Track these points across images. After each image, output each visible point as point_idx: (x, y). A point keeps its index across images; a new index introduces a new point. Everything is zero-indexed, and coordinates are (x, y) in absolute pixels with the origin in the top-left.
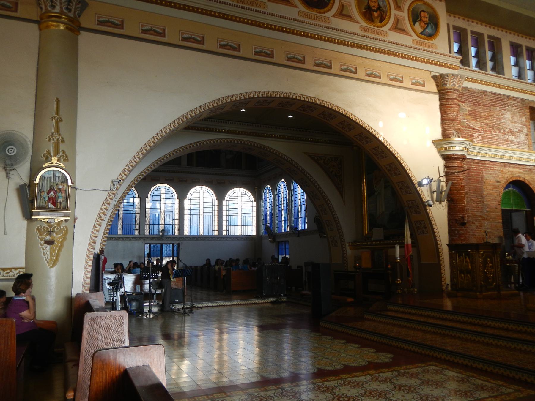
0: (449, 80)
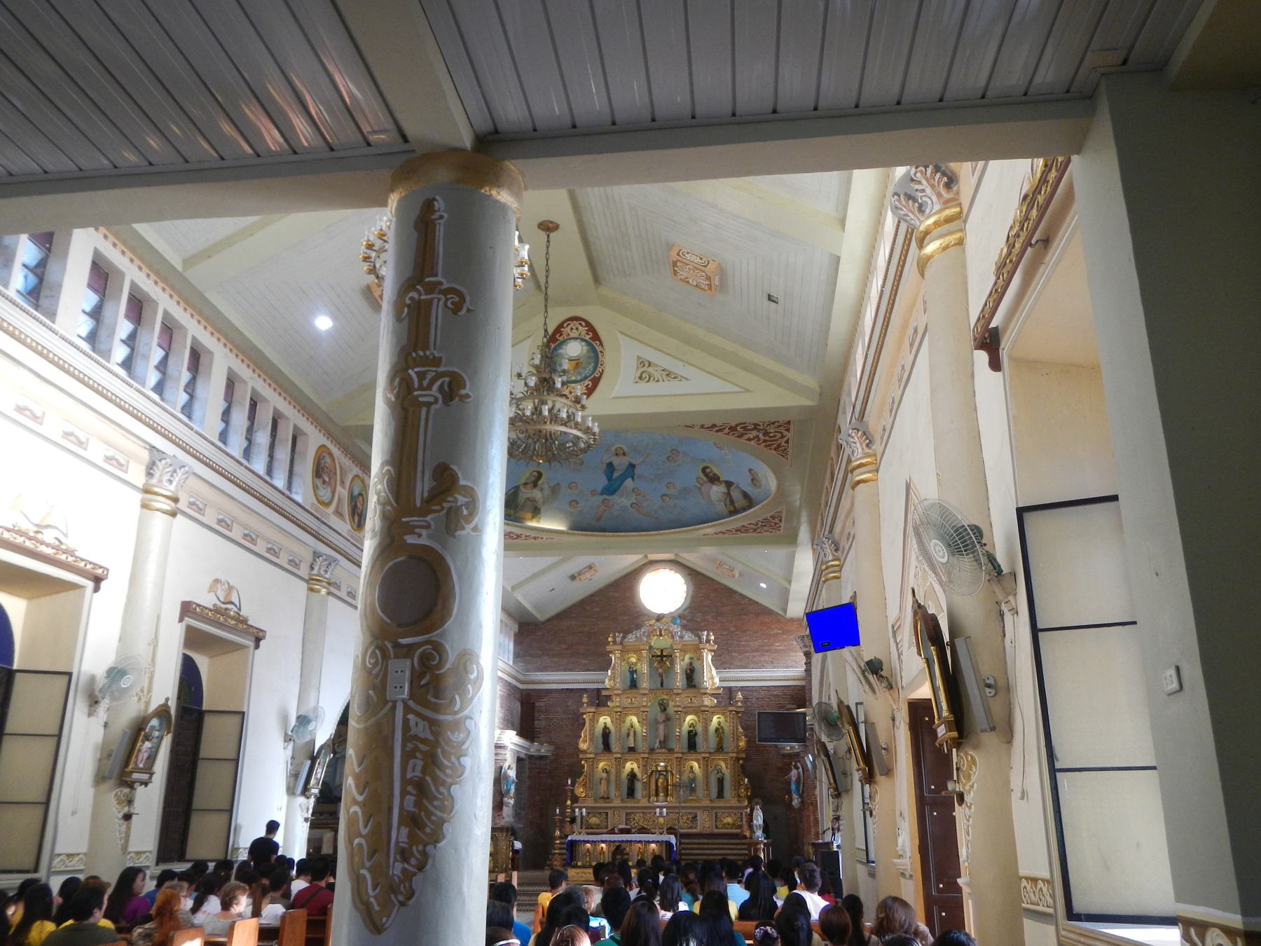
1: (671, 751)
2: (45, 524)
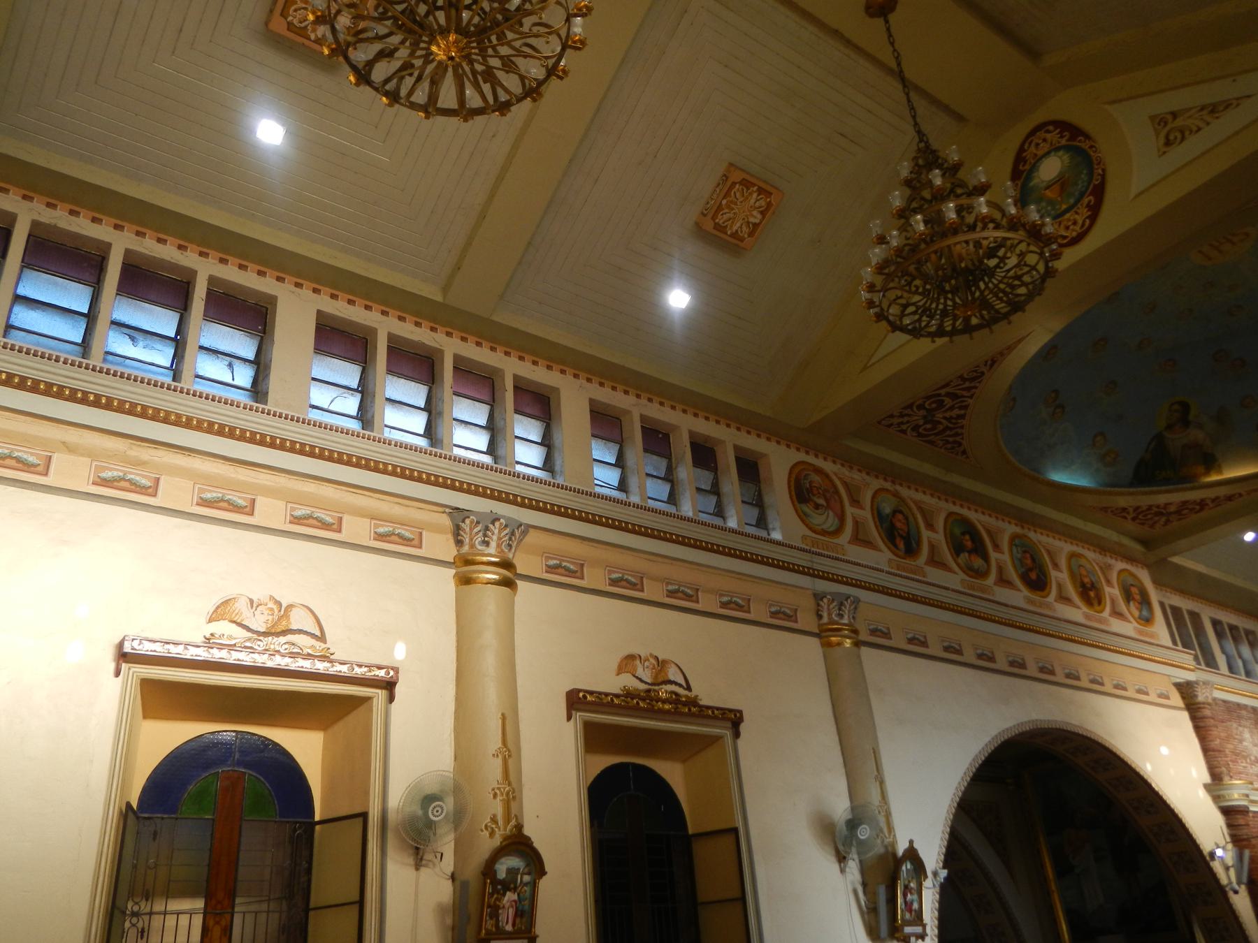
0: (1200, 690)
2: (279, 630)
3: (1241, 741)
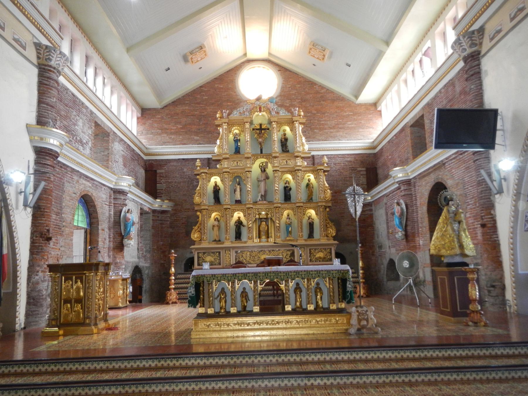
1: (271, 202)
3: (75, 125)
